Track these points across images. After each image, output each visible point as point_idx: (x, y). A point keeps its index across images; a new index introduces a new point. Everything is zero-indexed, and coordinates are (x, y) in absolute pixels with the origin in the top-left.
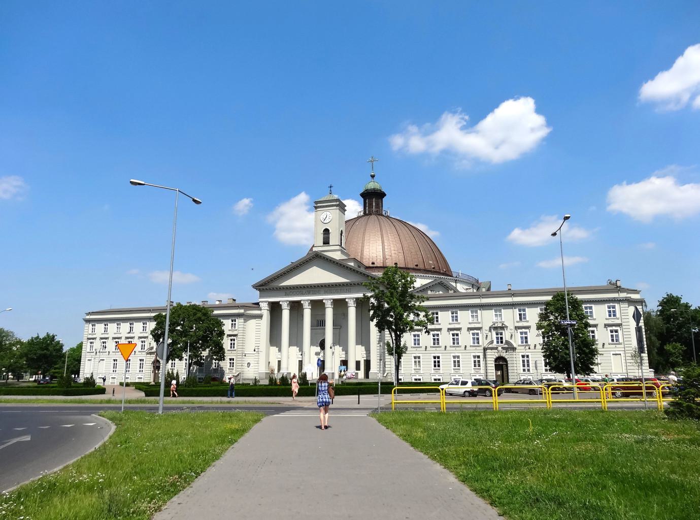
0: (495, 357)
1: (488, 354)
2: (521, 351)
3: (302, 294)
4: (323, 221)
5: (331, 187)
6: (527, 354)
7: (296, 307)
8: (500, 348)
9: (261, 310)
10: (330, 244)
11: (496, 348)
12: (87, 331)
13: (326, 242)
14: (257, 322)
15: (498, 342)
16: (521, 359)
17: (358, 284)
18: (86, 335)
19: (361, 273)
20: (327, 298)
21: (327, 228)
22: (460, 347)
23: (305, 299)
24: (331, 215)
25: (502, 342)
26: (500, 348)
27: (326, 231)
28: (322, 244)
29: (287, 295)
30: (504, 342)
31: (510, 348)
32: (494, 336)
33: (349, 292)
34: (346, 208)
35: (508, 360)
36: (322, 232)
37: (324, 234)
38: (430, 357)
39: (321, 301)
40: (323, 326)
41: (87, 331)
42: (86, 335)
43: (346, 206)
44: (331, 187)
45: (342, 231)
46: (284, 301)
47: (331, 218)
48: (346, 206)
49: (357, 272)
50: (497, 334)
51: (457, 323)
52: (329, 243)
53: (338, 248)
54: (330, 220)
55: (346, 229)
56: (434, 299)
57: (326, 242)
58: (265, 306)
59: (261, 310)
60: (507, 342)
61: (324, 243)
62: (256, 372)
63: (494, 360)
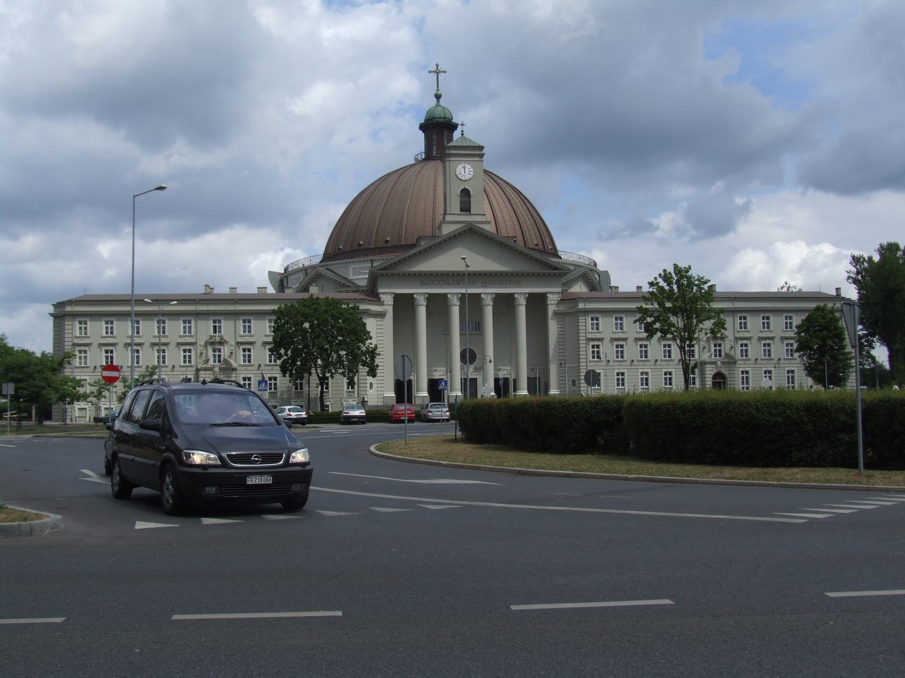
0: (713, 374)
1: (707, 369)
2: (740, 367)
3: (448, 284)
4: (460, 176)
6: (747, 369)
7: (438, 305)
8: (719, 363)
9: (382, 304)
10: (472, 212)
11: (715, 363)
12: (71, 331)
13: (466, 208)
14: (379, 323)
15: (716, 356)
16: (741, 375)
17: (528, 274)
18: (70, 339)
20: (488, 292)
22: (772, 359)
23: (453, 292)
24: (472, 169)
25: (720, 356)
26: (719, 363)
28: (459, 212)
29: (423, 284)
30: (723, 354)
31: (731, 362)
32: (713, 348)
33: (518, 284)
35: (728, 376)
36: (459, 193)
37: (461, 196)
38: (660, 373)
39: (445, 295)
40: (479, 330)
41: (71, 331)
42: (70, 339)
46: (420, 292)
47: (472, 173)
50: (715, 346)
51: (745, 332)
52: (469, 211)
54: (470, 177)
56: (618, 299)
57: (466, 208)
58: (388, 300)
59: (382, 304)
60: (727, 355)
61: (461, 210)
62: (379, 396)
63: (712, 376)
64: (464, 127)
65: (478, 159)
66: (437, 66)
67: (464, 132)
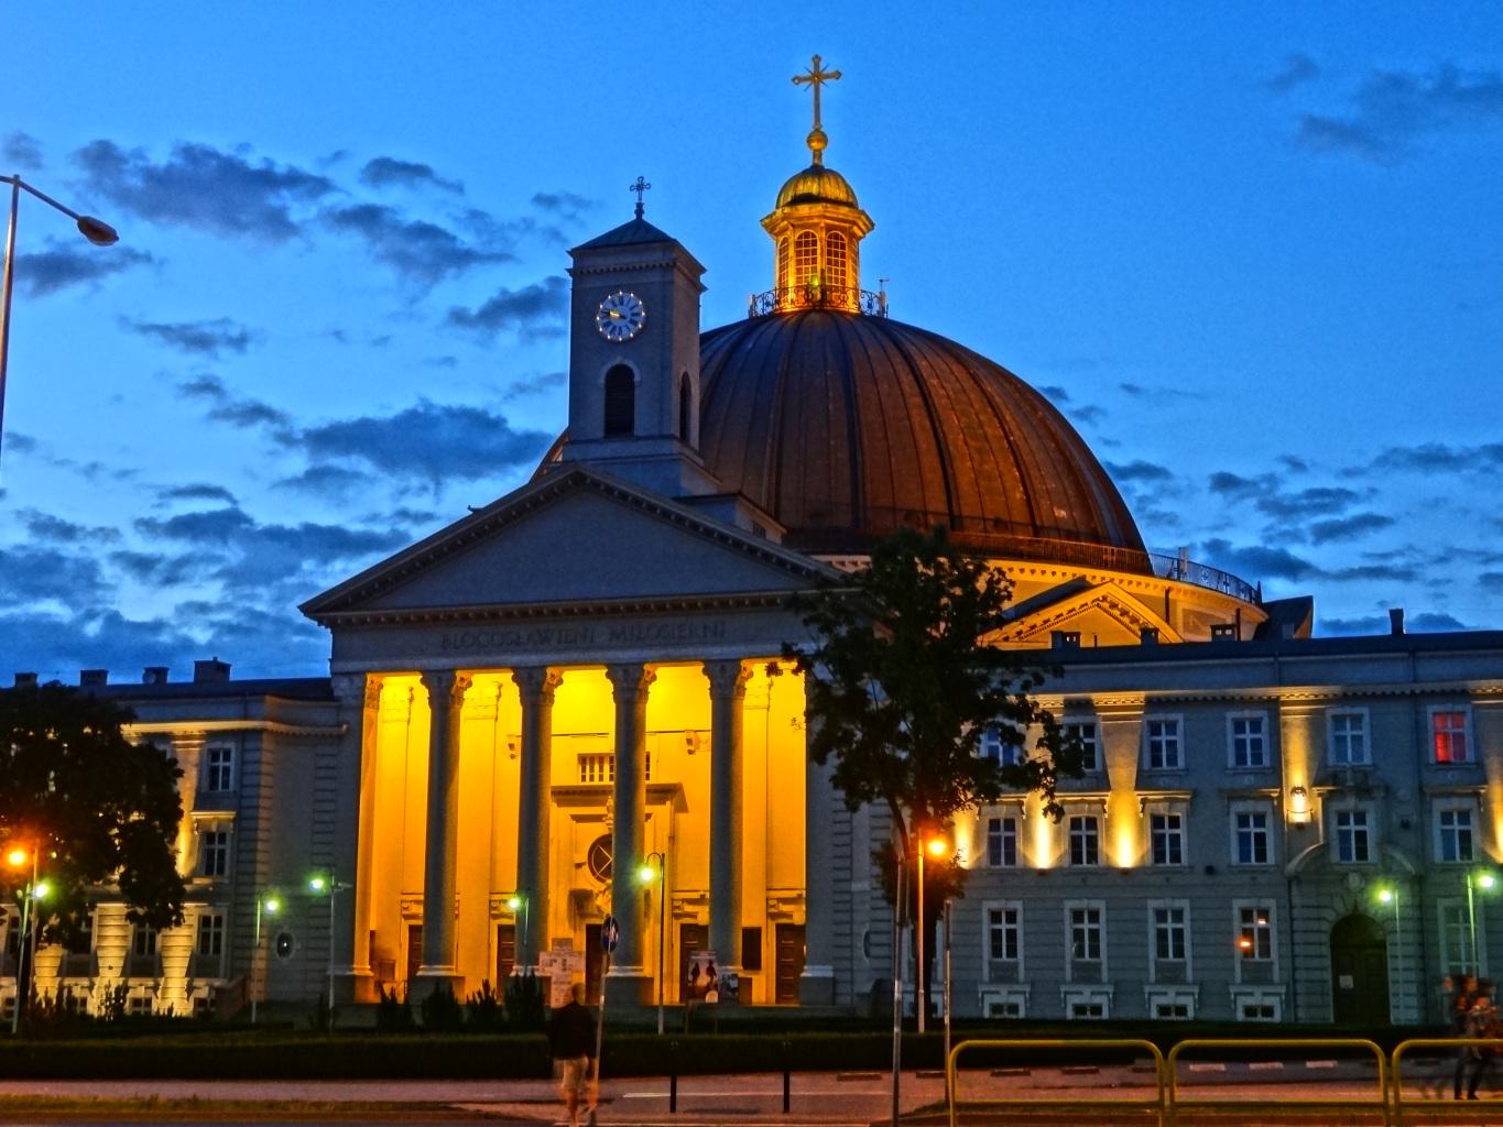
5: (640, 187)
10: (638, 431)
13: (619, 423)
19: (767, 556)
21: (631, 364)
27: (620, 380)
34: (703, 279)
36: (602, 381)
43: (703, 270)
44: (640, 187)
45: (686, 377)
48: (703, 270)
49: (752, 550)
53: (676, 447)
55: (702, 371)
57: (619, 423)
64: (645, 192)
65: (655, 277)
66: (817, 59)
67: (644, 208)
